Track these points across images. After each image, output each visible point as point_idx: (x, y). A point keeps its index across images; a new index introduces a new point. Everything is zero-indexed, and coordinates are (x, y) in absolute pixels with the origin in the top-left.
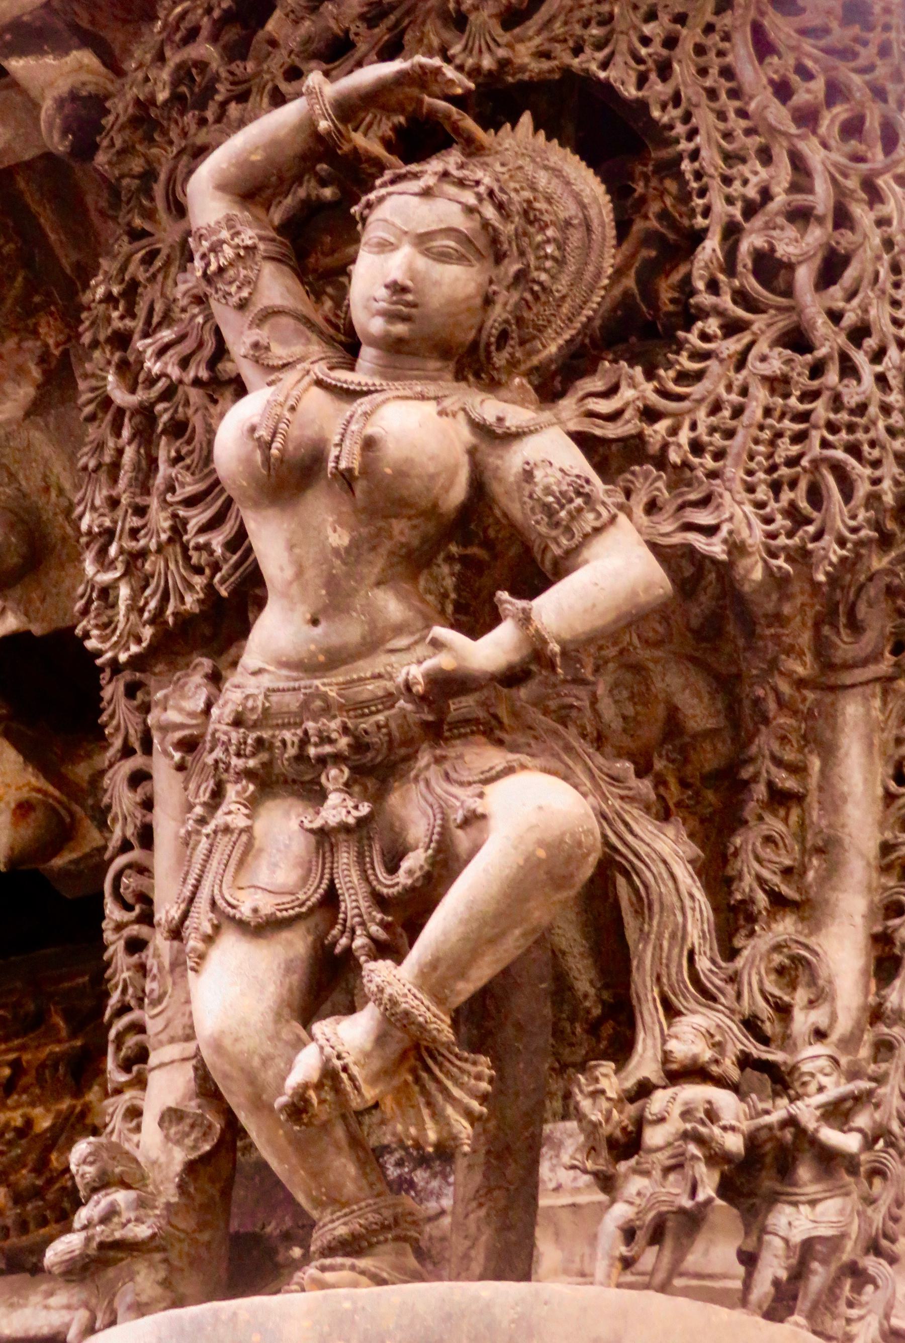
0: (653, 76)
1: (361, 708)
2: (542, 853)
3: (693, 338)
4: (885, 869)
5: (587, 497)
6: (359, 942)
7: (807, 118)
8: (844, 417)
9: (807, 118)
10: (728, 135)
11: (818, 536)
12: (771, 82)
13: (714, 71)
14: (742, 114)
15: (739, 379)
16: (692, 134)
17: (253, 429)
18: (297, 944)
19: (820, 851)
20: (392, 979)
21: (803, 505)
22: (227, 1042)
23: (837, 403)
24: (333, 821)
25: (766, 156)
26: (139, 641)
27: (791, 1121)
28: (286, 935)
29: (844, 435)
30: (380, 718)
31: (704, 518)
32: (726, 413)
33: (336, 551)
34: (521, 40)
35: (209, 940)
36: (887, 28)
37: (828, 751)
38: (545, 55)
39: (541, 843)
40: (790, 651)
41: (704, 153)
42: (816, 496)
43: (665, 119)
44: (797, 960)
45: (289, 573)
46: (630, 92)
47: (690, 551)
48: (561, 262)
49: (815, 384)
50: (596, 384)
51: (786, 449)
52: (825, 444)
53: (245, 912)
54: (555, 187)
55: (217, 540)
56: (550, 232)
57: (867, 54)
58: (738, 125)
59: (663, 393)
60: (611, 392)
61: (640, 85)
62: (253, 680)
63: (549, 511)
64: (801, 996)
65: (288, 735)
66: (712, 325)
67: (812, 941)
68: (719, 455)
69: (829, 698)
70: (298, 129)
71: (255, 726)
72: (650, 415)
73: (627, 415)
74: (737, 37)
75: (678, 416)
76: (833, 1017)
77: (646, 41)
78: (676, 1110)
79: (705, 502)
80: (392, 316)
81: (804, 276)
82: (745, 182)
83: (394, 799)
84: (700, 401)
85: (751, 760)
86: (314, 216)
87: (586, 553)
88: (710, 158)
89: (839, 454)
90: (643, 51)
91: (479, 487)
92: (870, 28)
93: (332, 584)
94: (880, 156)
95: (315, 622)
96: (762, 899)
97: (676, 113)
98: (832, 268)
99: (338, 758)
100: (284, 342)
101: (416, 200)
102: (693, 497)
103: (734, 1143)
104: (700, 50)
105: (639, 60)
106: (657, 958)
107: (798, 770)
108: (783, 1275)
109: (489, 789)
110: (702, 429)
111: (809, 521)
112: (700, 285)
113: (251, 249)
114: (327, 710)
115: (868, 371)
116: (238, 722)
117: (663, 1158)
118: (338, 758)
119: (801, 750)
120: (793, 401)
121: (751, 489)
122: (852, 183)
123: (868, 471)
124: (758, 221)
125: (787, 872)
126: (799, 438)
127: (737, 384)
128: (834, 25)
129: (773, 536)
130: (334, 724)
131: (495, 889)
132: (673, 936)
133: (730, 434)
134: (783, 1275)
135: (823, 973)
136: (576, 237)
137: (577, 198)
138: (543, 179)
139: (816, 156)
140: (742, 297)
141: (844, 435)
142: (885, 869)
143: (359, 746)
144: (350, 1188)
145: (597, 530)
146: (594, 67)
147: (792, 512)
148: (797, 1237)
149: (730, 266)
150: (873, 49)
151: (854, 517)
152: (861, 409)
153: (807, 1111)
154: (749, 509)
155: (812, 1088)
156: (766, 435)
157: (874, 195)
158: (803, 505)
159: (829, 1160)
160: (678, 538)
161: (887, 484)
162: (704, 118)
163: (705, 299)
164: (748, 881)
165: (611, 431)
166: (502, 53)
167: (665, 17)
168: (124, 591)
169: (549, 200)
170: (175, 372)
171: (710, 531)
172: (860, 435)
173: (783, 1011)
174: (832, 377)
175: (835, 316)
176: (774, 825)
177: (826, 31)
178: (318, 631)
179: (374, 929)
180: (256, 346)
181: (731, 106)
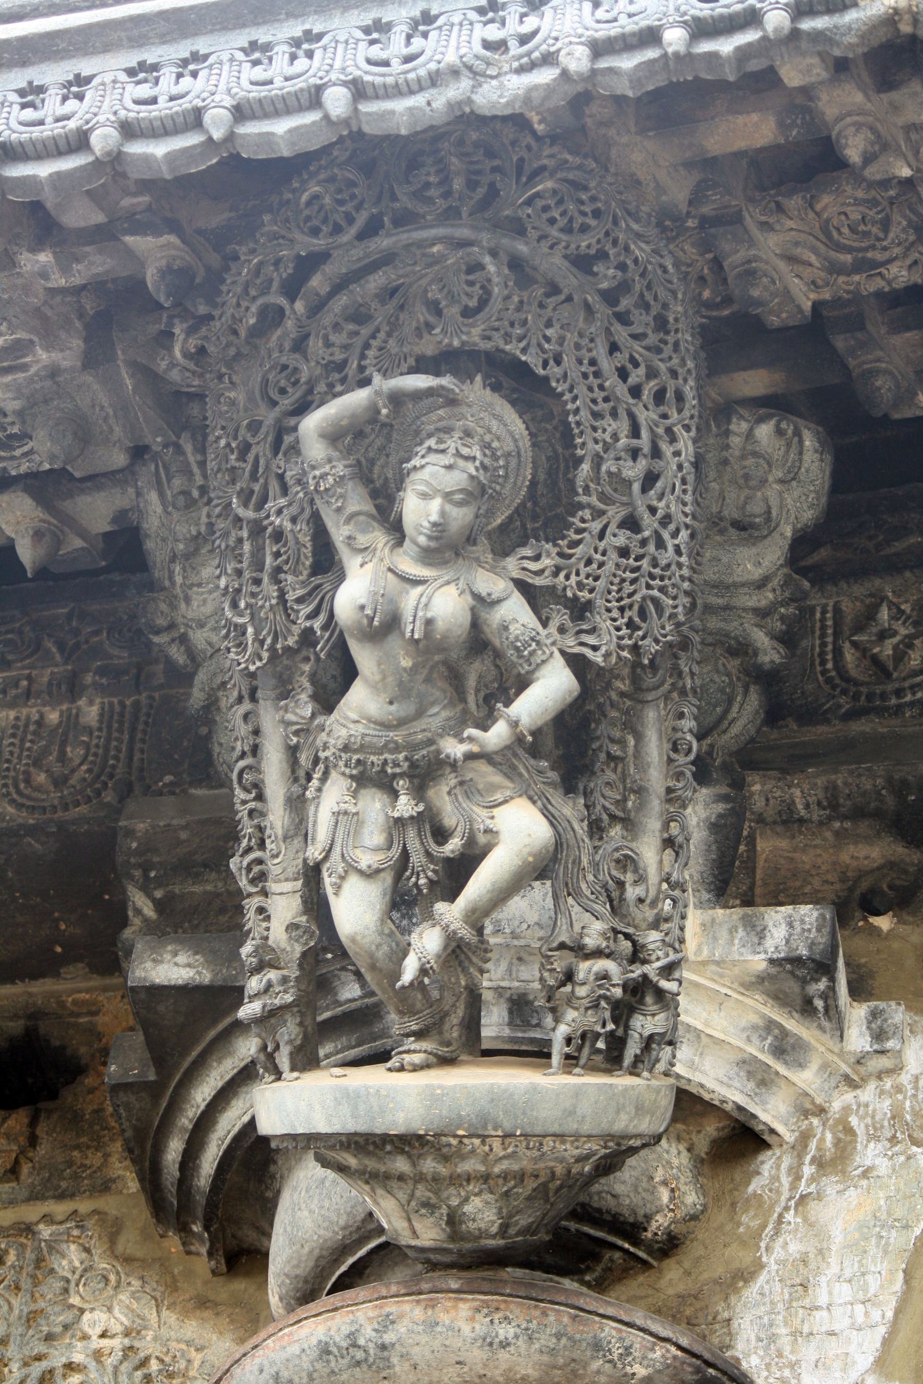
0: (551, 362)
1: (414, 747)
2: (531, 859)
3: (576, 520)
4: (669, 801)
5: (538, 643)
6: (422, 881)
7: (636, 392)
8: (657, 571)
9: (636, 392)
10: (594, 401)
11: (643, 638)
12: (617, 369)
13: (586, 362)
14: (601, 387)
15: (602, 545)
16: (575, 398)
17: (362, 608)
18: (388, 878)
19: (635, 792)
20: (451, 912)
21: (637, 619)
22: (359, 938)
23: (655, 563)
24: (406, 815)
25: (614, 414)
26: (261, 659)
27: (645, 976)
28: (382, 875)
29: (658, 582)
30: (424, 752)
31: (591, 640)
32: (595, 566)
33: (405, 669)
34: (473, 326)
35: (343, 878)
36: (677, 331)
37: (639, 738)
38: (489, 338)
39: (530, 854)
40: (617, 677)
41: (582, 413)
42: (643, 614)
43: (559, 390)
44: (626, 856)
45: (378, 677)
46: (541, 372)
47: (583, 656)
48: (506, 477)
49: (641, 551)
50: (528, 552)
51: (628, 588)
52: (649, 587)
53: (363, 865)
54: (502, 432)
55: (317, 624)
56: (501, 463)
57: (668, 350)
58: (599, 395)
59: (561, 555)
60: (537, 558)
61: (544, 368)
62: (351, 726)
63: (517, 649)
64: (629, 877)
65: (373, 758)
66: (587, 514)
67: (633, 845)
68: (591, 591)
69: (639, 706)
70: (365, 403)
71: (355, 751)
72: (557, 571)
73: (546, 573)
74: (598, 340)
75: (569, 567)
76: (647, 891)
77: (548, 339)
78: (592, 978)
79: (593, 631)
80: (430, 538)
81: (636, 487)
82: (604, 430)
83: (431, 793)
84: (580, 559)
85: (598, 738)
86: (377, 460)
87: (537, 674)
88: (584, 414)
89: (655, 593)
90: (546, 346)
91: (476, 624)
92: (667, 333)
93: (400, 684)
94: (675, 415)
95: (391, 703)
96: (605, 817)
97: (566, 386)
98: (650, 479)
99: (402, 775)
100: (364, 531)
101: (443, 470)
102: (584, 627)
103: (618, 992)
104: (578, 347)
105: (544, 351)
106: (565, 873)
107: (622, 742)
108: (638, 1052)
109: (496, 811)
110: (582, 576)
111: (639, 628)
112: (580, 491)
113: (342, 478)
114: (397, 749)
115: (670, 543)
116: (346, 748)
117: (585, 1002)
118: (402, 775)
119: (622, 730)
120: (631, 561)
121: (609, 610)
122: (660, 431)
123: (671, 602)
124: (612, 454)
125: (617, 802)
126: (633, 581)
127: (601, 549)
128: (649, 332)
129: (620, 638)
130: (401, 756)
131: (506, 876)
132: (574, 862)
133: (596, 579)
134: (638, 1052)
135: (641, 865)
136: (513, 462)
137: (511, 434)
138: (494, 425)
139: (643, 416)
140: (603, 497)
141: (658, 582)
142: (669, 801)
143: (413, 765)
144: (419, 1006)
145: (543, 662)
146: (518, 352)
147: (630, 624)
148: (646, 1033)
149: (597, 479)
150: (670, 346)
151: (663, 628)
152: (668, 566)
153: (651, 970)
154: (609, 622)
155: (653, 957)
156: (617, 580)
157: (673, 439)
158: (637, 619)
159: (660, 994)
160: (578, 650)
161: (680, 609)
162: (581, 390)
163: (584, 499)
164: (599, 808)
165: (538, 581)
166: (464, 338)
167: (557, 326)
168: (250, 630)
169: (498, 439)
170: (288, 525)
171: (595, 648)
172: (667, 582)
173: (621, 884)
174: (651, 548)
175: (653, 510)
176: (610, 775)
177: (644, 335)
178: (393, 708)
179: (430, 874)
180: (349, 538)
181: (595, 382)
